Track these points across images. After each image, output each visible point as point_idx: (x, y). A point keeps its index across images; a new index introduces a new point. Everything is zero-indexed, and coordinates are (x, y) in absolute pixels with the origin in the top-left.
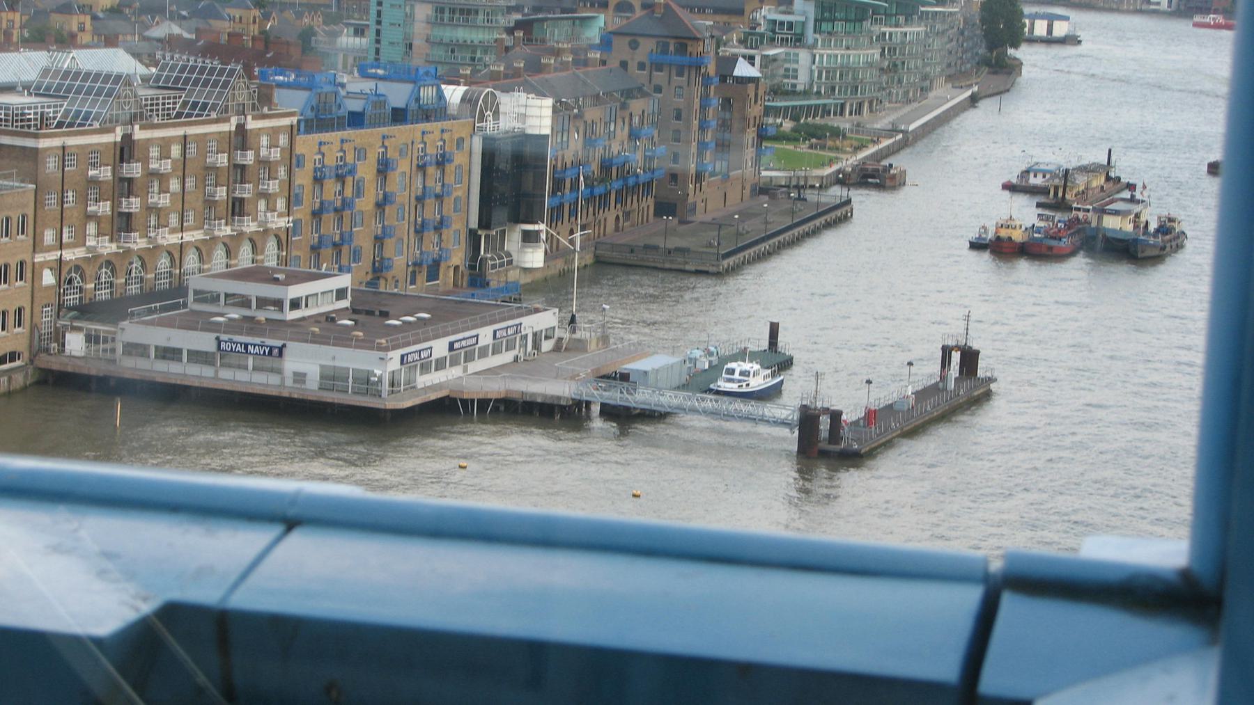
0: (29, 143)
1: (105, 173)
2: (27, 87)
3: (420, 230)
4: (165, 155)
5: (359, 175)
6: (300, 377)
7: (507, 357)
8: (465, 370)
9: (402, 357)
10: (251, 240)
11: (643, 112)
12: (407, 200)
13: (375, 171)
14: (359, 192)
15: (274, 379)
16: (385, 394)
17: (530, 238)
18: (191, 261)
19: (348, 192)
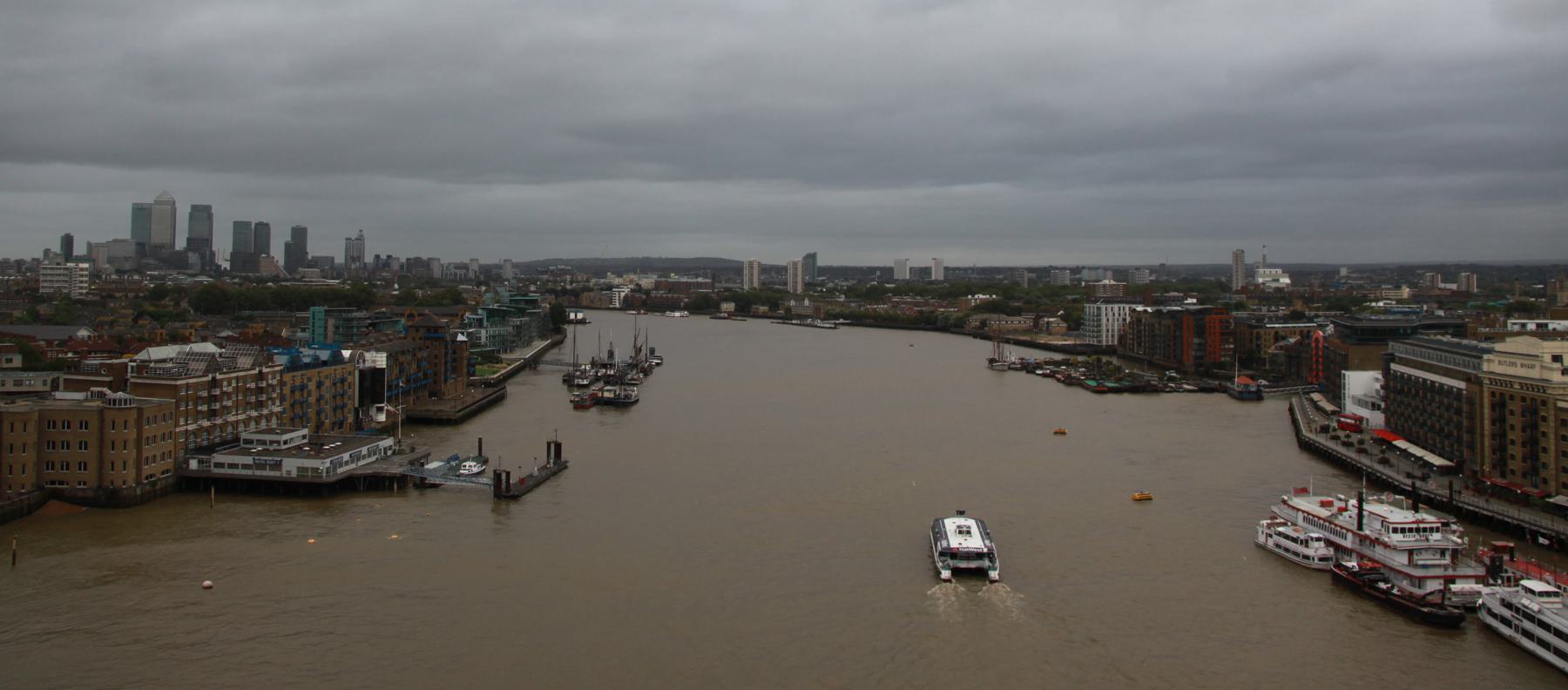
0: (173, 383)
1: (205, 394)
2: (171, 359)
3: (335, 410)
4: (229, 384)
5: (310, 387)
6: (289, 472)
7: (373, 459)
14: (309, 395)
15: (277, 474)
17: (380, 410)
18: (241, 428)
19: (305, 395)
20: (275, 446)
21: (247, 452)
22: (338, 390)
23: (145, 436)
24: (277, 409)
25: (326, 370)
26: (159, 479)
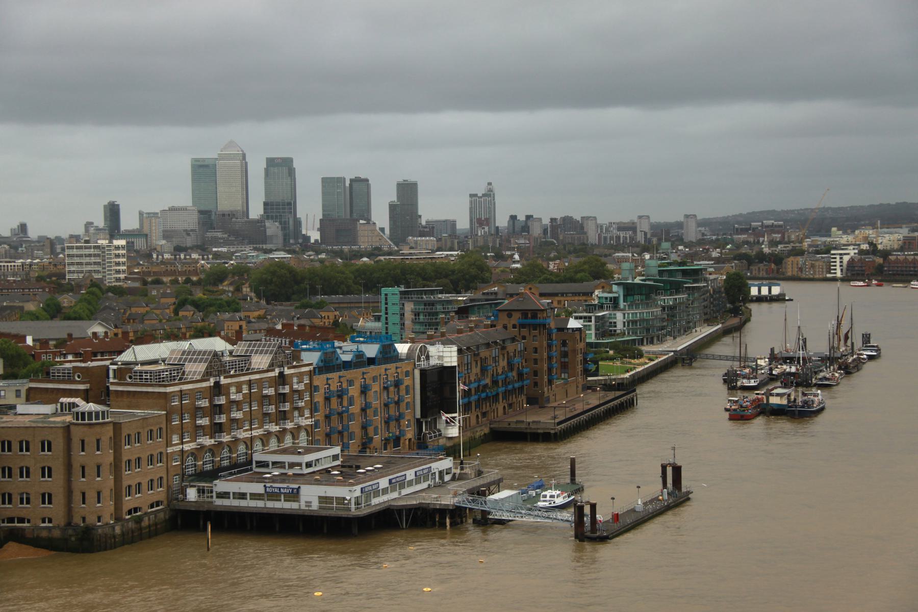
0: (162, 390)
1: (204, 403)
2: (164, 361)
3: (387, 423)
4: (239, 391)
7: (424, 485)
8: (400, 493)
9: (362, 489)
10: (291, 432)
11: (515, 350)
12: (379, 405)
13: (360, 392)
14: (351, 402)
16: (353, 510)
18: (258, 445)
19: (345, 403)
20: (297, 470)
21: (259, 478)
22: (391, 396)
23: (125, 459)
24: (306, 422)
25: (373, 370)
26: (146, 514)
